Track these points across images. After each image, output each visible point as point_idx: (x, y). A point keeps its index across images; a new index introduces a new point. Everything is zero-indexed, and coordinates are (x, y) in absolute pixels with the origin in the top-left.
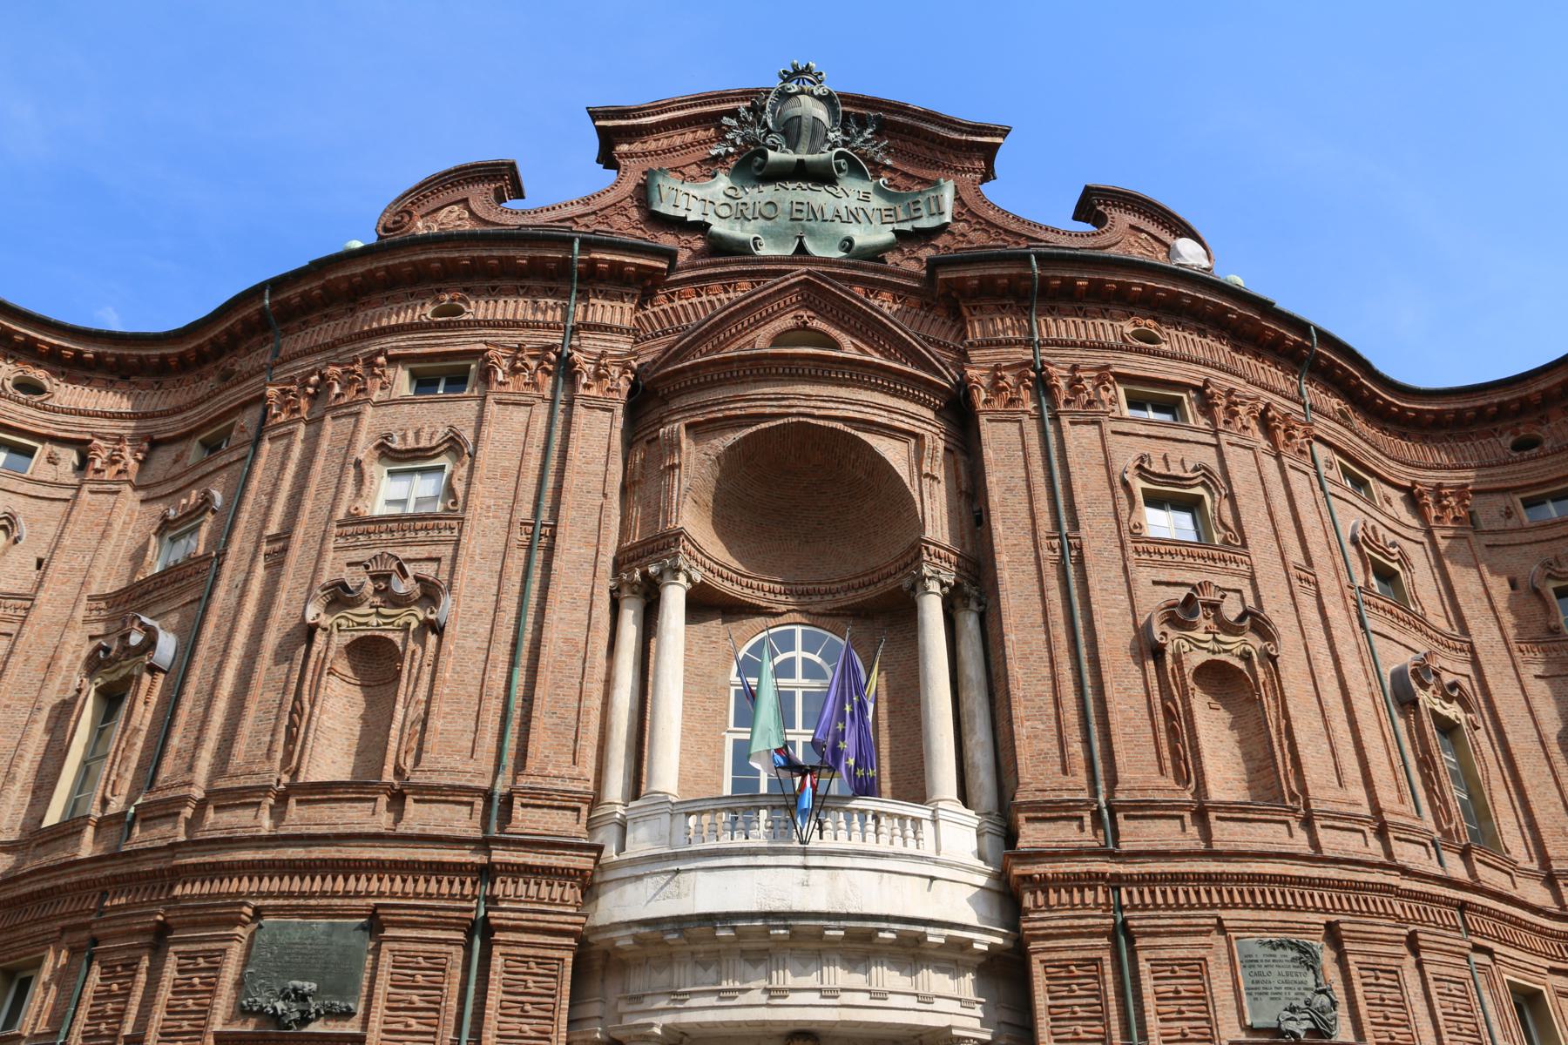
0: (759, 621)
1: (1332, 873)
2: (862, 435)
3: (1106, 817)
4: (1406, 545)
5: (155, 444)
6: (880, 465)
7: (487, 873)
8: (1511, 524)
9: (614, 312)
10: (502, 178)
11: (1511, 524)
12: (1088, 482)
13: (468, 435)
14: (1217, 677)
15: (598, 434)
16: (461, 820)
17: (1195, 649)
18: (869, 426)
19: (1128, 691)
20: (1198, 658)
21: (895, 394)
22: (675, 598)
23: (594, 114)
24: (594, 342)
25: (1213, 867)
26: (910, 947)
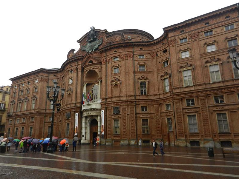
0: (94, 84)
1: (121, 101)
2: (94, 70)
3: (106, 99)
4: (146, 62)
5: (62, 77)
6: (95, 72)
7: (75, 108)
8: (161, 55)
9: (80, 63)
10: (73, 50)
11: (161, 55)
12: (109, 69)
13: (73, 76)
14: (116, 85)
15: (80, 74)
16: (73, 105)
17: (114, 83)
18: (95, 68)
19: (109, 88)
20: (114, 84)
21: (96, 65)
22: (85, 86)
23: (78, 41)
24: (79, 66)
25: (111, 102)
26: (94, 110)
